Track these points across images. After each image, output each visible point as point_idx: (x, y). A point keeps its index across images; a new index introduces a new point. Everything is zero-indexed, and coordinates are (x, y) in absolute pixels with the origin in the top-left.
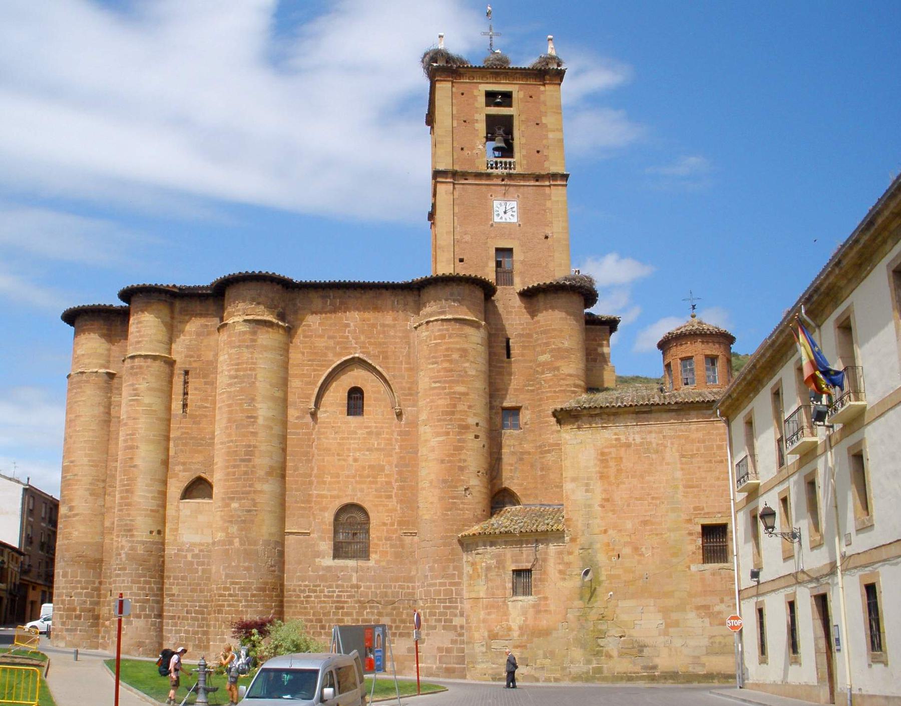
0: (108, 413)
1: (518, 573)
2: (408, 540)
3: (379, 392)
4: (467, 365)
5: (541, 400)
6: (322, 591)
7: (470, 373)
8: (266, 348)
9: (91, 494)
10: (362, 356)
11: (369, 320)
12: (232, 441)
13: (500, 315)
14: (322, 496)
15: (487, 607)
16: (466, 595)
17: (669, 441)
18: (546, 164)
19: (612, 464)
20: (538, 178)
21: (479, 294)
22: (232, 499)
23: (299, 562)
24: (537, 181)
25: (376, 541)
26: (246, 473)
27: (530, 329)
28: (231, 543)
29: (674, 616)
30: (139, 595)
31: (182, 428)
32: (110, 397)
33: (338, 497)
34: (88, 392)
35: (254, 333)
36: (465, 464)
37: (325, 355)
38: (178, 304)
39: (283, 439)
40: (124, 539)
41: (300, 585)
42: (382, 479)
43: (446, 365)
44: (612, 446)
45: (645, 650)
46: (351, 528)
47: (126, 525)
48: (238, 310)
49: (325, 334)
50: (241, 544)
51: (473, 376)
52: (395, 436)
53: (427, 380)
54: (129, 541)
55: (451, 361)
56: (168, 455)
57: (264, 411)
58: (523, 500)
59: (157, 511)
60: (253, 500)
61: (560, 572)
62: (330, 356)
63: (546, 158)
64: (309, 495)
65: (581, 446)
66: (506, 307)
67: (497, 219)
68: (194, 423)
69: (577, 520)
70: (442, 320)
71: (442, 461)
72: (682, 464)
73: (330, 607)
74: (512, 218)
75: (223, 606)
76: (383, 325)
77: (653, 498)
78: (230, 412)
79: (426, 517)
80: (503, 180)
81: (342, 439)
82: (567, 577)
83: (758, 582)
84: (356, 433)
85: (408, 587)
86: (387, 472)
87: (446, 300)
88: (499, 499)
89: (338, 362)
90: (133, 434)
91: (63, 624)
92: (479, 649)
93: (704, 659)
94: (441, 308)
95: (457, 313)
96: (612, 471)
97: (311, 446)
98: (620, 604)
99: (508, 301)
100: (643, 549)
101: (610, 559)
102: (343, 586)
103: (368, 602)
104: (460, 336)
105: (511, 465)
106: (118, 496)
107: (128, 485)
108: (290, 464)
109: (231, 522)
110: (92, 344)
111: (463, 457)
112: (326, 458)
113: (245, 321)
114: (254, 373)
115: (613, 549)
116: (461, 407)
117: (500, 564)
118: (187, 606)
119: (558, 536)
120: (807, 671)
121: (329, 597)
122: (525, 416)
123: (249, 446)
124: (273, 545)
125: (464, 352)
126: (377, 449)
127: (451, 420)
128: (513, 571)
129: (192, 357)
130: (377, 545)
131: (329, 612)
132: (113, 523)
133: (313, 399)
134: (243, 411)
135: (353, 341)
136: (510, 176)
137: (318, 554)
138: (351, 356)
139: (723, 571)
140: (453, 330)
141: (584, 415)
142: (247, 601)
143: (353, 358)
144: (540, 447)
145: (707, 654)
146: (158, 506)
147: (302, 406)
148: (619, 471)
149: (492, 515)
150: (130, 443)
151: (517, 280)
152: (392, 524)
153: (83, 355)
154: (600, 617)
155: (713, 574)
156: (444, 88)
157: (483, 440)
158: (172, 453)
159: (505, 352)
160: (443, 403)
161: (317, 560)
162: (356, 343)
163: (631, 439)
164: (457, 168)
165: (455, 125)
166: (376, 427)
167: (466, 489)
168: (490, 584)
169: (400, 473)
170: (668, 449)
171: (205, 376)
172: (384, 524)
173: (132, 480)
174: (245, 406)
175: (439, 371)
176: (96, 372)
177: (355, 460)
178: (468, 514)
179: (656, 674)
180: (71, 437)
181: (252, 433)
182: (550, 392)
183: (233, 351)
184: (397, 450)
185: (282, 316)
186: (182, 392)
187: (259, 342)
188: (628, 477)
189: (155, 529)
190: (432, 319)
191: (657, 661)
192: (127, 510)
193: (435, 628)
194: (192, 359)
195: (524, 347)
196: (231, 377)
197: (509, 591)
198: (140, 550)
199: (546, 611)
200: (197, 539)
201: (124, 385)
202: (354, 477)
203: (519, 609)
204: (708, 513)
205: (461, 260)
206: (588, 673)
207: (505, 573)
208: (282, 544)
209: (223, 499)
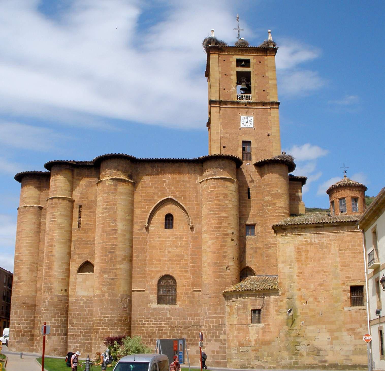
0: (39, 228)
1: (254, 311)
2: (196, 294)
3: (181, 216)
4: (227, 202)
5: (266, 220)
6: (151, 321)
7: (229, 206)
8: (121, 193)
9: (30, 271)
10: (172, 197)
11: (176, 178)
13: (244, 176)
15: (238, 330)
16: (227, 323)
17: (333, 242)
18: (268, 97)
19: (303, 254)
20: (264, 104)
21: (234, 165)
22: (105, 272)
23: (139, 306)
24: (264, 106)
25: (180, 295)
26: (111, 259)
27: (260, 183)
28: (104, 296)
29: (336, 334)
30: (55, 323)
32: (40, 220)
33: (160, 271)
34: (29, 217)
35: (116, 186)
36: (227, 254)
37: (153, 197)
38: (76, 171)
39: (131, 241)
40: (47, 294)
41: (140, 318)
42: (183, 262)
44: (303, 244)
45: (321, 352)
46: (167, 288)
47: (48, 286)
48: (108, 174)
49: (153, 186)
50: (109, 297)
51: (231, 208)
52: (190, 238)
53: (206, 210)
54: (50, 295)
55: (219, 200)
56: (70, 250)
57: (121, 226)
58: (257, 273)
59: (65, 279)
60: (115, 273)
61: (276, 311)
62: (156, 198)
64: (145, 270)
65: (287, 245)
66: (247, 171)
67: (242, 126)
68: (84, 233)
69: (285, 284)
70: (214, 179)
71: (215, 253)
72: (340, 254)
73: (155, 329)
74: (251, 125)
75: (99, 329)
76: (183, 181)
77: (325, 272)
78: (103, 227)
79: (207, 282)
80: (246, 105)
81: (163, 241)
82: (280, 314)
83: (380, 316)
84: (169, 238)
85: (197, 319)
87: (216, 168)
88: (244, 272)
89: (160, 201)
90: (53, 239)
91: (15, 339)
92: (233, 351)
93: (351, 357)
94: (214, 172)
95: (222, 175)
96: (303, 258)
97: (145, 245)
98: (307, 327)
99: (249, 168)
100: (320, 299)
101: (302, 304)
102: (162, 318)
103: (176, 327)
104: (223, 187)
105: (251, 255)
106: (44, 271)
107: (49, 265)
108: (134, 254)
109: (103, 285)
110: (31, 191)
111: (225, 250)
112: (154, 251)
113: (111, 179)
114: (116, 206)
116: (224, 224)
117: (245, 307)
118: (80, 329)
119: (274, 292)
121: (155, 324)
122: (258, 229)
123: (114, 245)
124: (125, 297)
125: (226, 196)
126: (180, 246)
127: (219, 231)
128: (252, 310)
129: (83, 198)
130: (180, 297)
131: (155, 332)
132: (42, 286)
133: (147, 220)
134: (110, 226)
135: (168, 190)
136: (249, 103)
138: (167, 198)
139: (361, 311)
140: (220, 183)
141: (289, 228)
142: (112, 326)
143: (168, 199)
144: (266, 245)
145: (353, 354)
146: (65, 276)
147: (141, 224)
148: (307, 258)
149: (240, 281)
150: (50, 244)
151: (253, 157)
152: (188, 286)
153: (26, 197)
154: (297, 334)
155: (356, 312)
156: (214, 57)
157: (236, 242)
158: (73, 248)
159: (247, 195)
161: (149, 305)
164: (222, 99)
166: (180, 235)
167: (227, 267)
168: (239, 317)
169: (192, 259)
170: (332, 246)
171: (90, 208)
172: (184, 286)
173: (52, 263)
175: (212, 205)
177: (169, 252)
178: (228, 281)
179: (327, 365)
180: (19, 240)
181: (115, 238)
182: (271, 216)
183: (105, 195)
184: (191, 247)
185: (130, 177)
186: (78, 216)
187: (118, 190)
188: (312, 261)
189: (63, 288)
190: (209, 178)
191: (327, 358)
192: (49, 279)
193: (210, 340)
194: (83, 199)
195: (257, 193)
196: (104, 209)
197: (249, 321)
199: (269, 331)
200: (86, 294)
201: (47, 213)
202: (168, 261)
204: (353, 280)
205: (224, 147)
206: (290, 364)
207: (247, 311)
208: (131, 297)
209: (100, 273)
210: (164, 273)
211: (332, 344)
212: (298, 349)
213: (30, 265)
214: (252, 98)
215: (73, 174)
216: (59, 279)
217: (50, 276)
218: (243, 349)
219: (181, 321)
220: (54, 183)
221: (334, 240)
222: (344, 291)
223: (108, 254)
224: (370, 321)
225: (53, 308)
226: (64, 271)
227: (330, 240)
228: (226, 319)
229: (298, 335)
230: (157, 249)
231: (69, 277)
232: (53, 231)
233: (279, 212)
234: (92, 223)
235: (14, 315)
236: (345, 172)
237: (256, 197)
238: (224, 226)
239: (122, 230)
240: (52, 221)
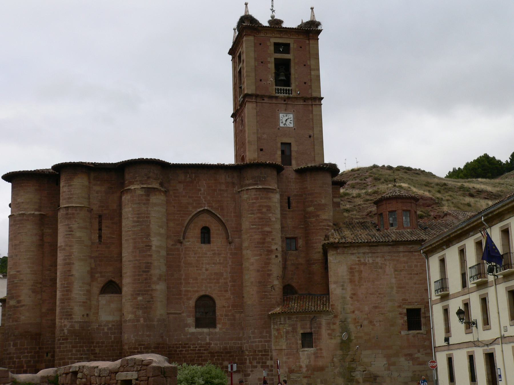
1: (304, 335)
2: (237, 316)
6: (189, 347)
9: (33, 292)
10: (209, 209)
12: (137, 260)
14: (187, 291)
15: (287, 355)
16: (273, 347)
19: (356, 274)
20: (305, 99)
22: (138, 294)
24: (305, 101)
26: (146, 279)
28: (138, 321)
32: (43, 230)
33: (197, 291)
35: (148, 195)
38: (92, 175)
41: (177, 344)
42: (222, 281)
43: (259, 215)
47: (67, 312)
48: (137, 181)
52: (229, 254)
54: (70, 322)
55: (262, 213)
60: (151, 295)
61: (329, 334)
62: (190, 208)
63: (310, 87)
64: (181, 291)
69: (338, 306)
71: (258, 271)
72: (395, 275)
74: (290, 124)
79: (249, 303)
80: (285, 101)
81: (199, 257)
83: (448, 343)
84: (206, 254)
85: (238, 344)
86: (225, 276)
89: (195, 212)
90: (71, 256)
96: (357, 278)
100: (375, 322)
101: (356, 327)
103: (216, 353)
107: (67, 287)
109: (138, 308)
111: (270, 268)
113: (142, 188)
115: (358, 322)
116: (268, 240)
117: (294, 330)
123: (148, 263)
126: (220, 263)
128: (302, 333)
131: (194, 360)
135: (203, 200)
136: (289, 98)
138: (202, 209)
139: (419, 335)
143: (204, 210)
148: (361, 278)
151: (294, 162)
152: (229, 307)
153: (23, 203)
155: (414, 336)
160: (257, 237)
161: (186, 329)
162: (205, 201)
164: (258, 93)
165: (256, 65)
166: (218, 250)
168: (288, 341)
170: (387, 267)
172: (224, 307)
174: (144, 239)
175: (255, 219)
176: (34, 214)
177: (207, 270)
183: (135, 206)
185: (161, 184)
187: (151, 201)
190: (250, 188)
193: (256, 367)
194: (104, 208)
196: (134, 222)
198: (77, 327)
199: (321, 356)
200: (110, 318)
203: (305, 356)
204: (410, 303)
205: (261, 150)
210: (202, 293)
211: (390, 370)
212: (354, 375)
213: (32, 286)
214: (291, 91)
215: (89, 179)
216: (80, 302)
217: (69, 299)
218: (293, 376)
219: (221, 346)
220: (68, 189)
222: (400, 314)
223: (142, 273)
224: (434, 347)
225: (74, 337)
226: (85, 292)
227: (385, 260)
228: (273, 344)
229: (353, 360)
231: (90, 299)
232: (70, 246)
233: (323, 225)
234: (115, 236)
235: (12, 347)
240: (69, 234)
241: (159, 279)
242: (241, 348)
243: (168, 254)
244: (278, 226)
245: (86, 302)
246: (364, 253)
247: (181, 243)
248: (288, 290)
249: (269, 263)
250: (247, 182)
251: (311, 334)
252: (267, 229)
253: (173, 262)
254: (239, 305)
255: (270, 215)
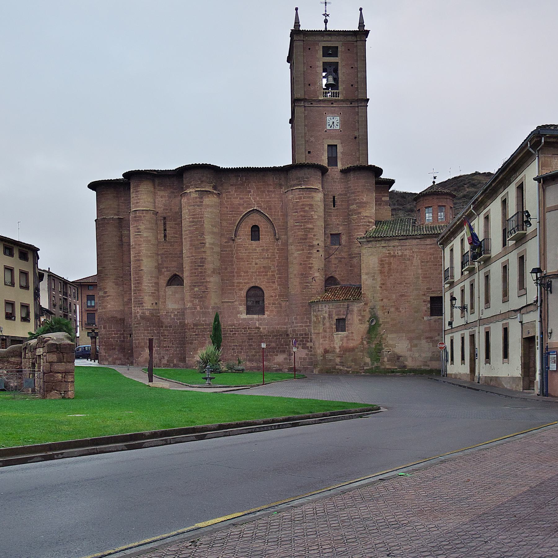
2: (283, 304)
14: (238, 283)
19: (386, 266)
22: (195, 286)
28: (195, 308)
29: (415, 342)
31: (164, 249)
35: (202, 198)
37: (239, 208)
38: (157, 182)
53: (292, 221)
55: (304, 211)
61: (360, 320)
67: (328, 128)
68: (171, 246)
78: (191, 241)
81: (249, 253)
84: (256, 250)
90: (140, 253)
93: (429, 363)
97: (233, 257)
101: (384, 313)
109: (194, 298)
111: (311, 262)
116: (310, 236)
120: (465, 369)
121: (244, 334)
123: (203, 258)
129: (167, 210)
134: (198, 240)
137: (239, 312)
147: (228, 236)
148: (390, 269)
155: (435, 321)
163: (396, 253)
169: (279, 270)
173: (140, 277)
177: (256, 264)
185: (215, 188)
200: (176, 306)
209: (190, 286)
210: (252, 285)
221: (416, 252)
230: (245, 261)
231: (158, 291)
236: (435, 178)
237: (342, 205)
238: (310, 238)
239: (210, 244)
241: (213, 272)
242: (287, 331)
243: (221, 251)
244: (321, 223)
245: (155, 293)
246: (394, 246)
247: (233, 240)
248: (330, 281)
249: (310, 257)
250: (292, 183)
251: (344, 320)
252: (310, 226)
253: (227, 258)
254: (285, 295)
255: (313, 213)
